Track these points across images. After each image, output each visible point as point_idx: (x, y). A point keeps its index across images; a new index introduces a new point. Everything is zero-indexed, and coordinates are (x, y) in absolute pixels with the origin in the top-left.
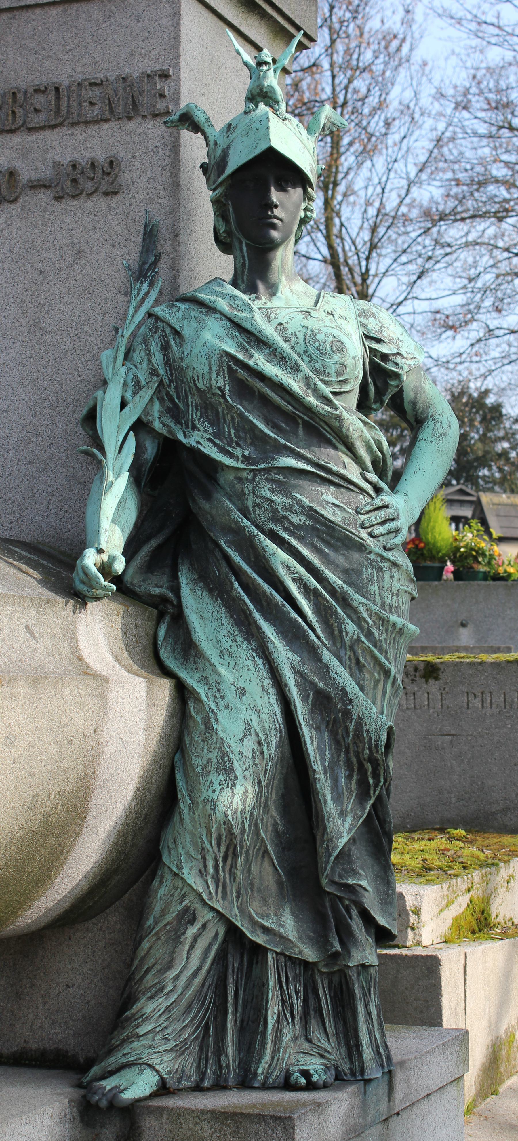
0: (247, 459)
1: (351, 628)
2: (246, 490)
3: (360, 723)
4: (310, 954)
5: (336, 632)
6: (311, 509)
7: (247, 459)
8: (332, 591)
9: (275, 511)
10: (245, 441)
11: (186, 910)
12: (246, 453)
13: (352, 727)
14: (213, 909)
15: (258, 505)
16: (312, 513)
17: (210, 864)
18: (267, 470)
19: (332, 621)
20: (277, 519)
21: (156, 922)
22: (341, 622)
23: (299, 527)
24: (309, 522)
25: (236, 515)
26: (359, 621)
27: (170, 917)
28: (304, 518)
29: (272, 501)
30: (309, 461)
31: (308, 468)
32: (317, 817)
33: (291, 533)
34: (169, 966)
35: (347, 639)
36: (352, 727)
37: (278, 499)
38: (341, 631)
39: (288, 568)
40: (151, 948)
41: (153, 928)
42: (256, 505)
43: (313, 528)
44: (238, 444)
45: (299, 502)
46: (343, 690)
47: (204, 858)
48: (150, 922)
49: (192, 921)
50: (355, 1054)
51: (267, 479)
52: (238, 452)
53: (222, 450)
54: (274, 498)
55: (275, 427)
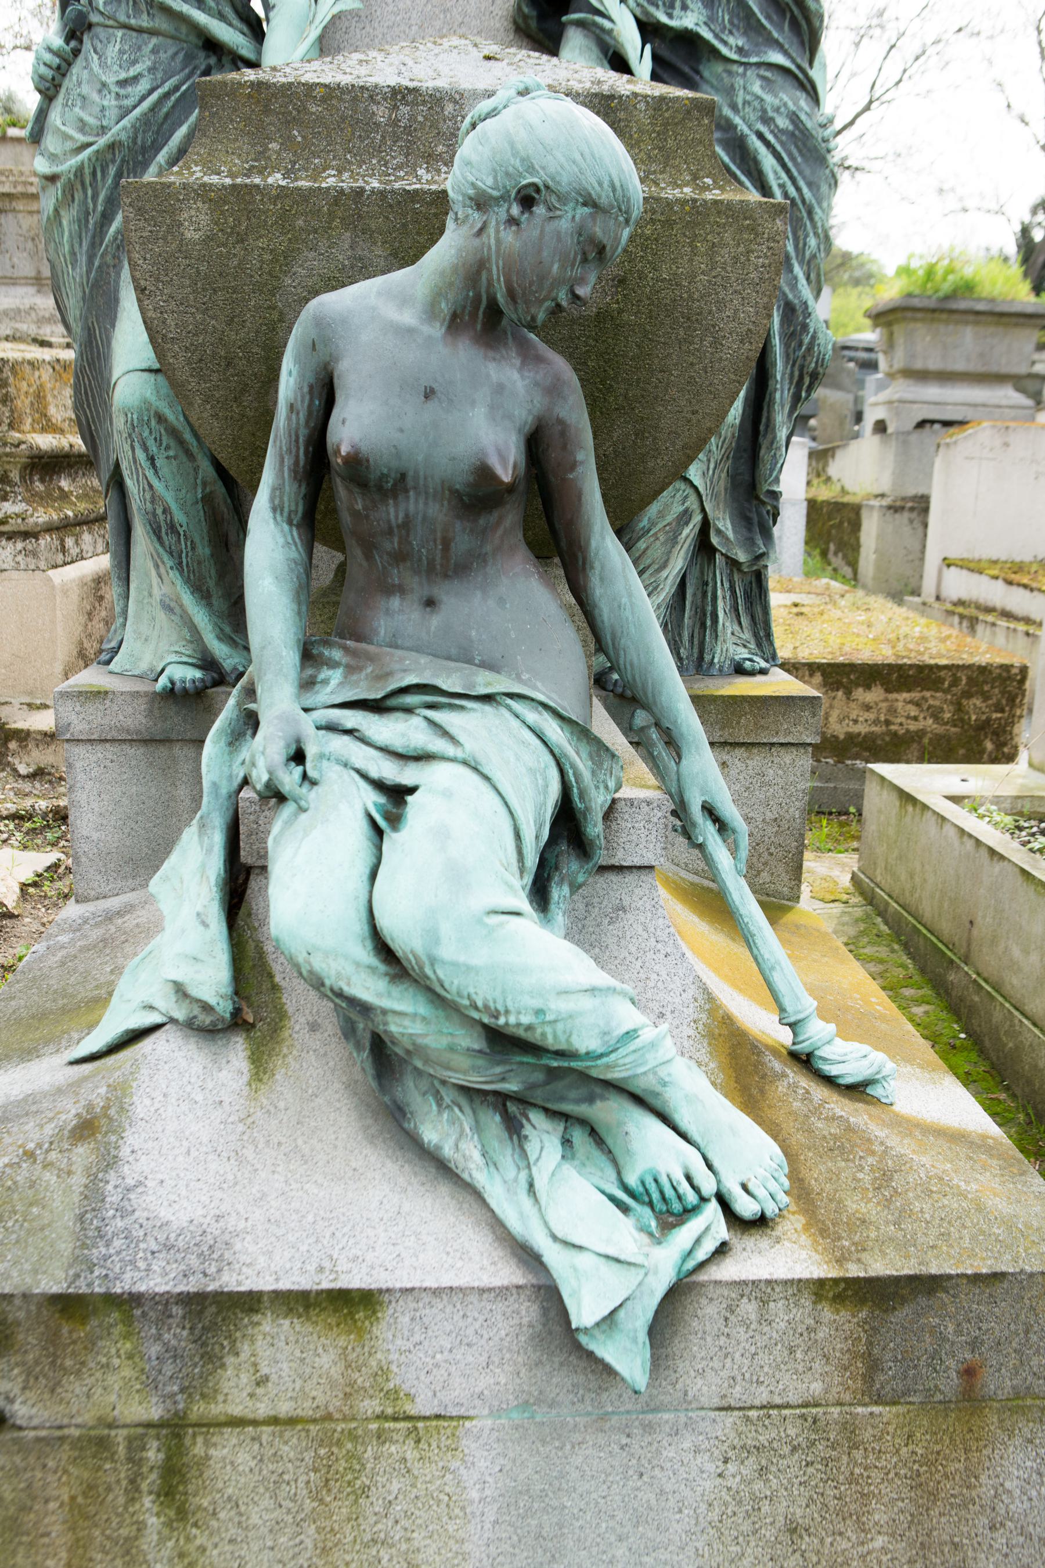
0: (740, 50)
1: (812, 242)
2: (737, 86)
3: (814, 337)
4: (742, 556)
5: (801, 245)
6: (794, 113)
7: (740, 50)
8: (804, 201)
9: (764, 111)
10: (738, 29)
11: (686, 511)
12: (740, 44)
13: (807, 340)
14: (703, 510)
15: (749, 103)
16: (794, 118)
17: (712, 466)
18: (759, 65)
19: (800, 233)
20: (766, 120)
21: (653, 524)
22: (807, 236)
23: (782, 131)
24: (791, 128)
25: (727, 112)
26: (816, 234)
27: (669, 518)
28: (787, 122)
29: (762, 100)
30: (793, 61)
31: (793, 67)
32: (767, 426)
33: (776, 136)
34: (664, 566)
35: (808, 254)
36: (807, 340)
37: (768, 98)
38: (805, 244)
39: (776, 173)
40: (647, 548)
41: (649, 530)
42: (745, 102)
43: (793, 134)
44: (731, 32)
45: (785, 104)
46: (805, 303)
47: (709, 460)
48: (645, 522)
49: (687, 524)
50: (765, 643)
51: (758, 75)
52: (731, 40)
53: (716, 36)
54: (765, 96)
55: (768, 17)
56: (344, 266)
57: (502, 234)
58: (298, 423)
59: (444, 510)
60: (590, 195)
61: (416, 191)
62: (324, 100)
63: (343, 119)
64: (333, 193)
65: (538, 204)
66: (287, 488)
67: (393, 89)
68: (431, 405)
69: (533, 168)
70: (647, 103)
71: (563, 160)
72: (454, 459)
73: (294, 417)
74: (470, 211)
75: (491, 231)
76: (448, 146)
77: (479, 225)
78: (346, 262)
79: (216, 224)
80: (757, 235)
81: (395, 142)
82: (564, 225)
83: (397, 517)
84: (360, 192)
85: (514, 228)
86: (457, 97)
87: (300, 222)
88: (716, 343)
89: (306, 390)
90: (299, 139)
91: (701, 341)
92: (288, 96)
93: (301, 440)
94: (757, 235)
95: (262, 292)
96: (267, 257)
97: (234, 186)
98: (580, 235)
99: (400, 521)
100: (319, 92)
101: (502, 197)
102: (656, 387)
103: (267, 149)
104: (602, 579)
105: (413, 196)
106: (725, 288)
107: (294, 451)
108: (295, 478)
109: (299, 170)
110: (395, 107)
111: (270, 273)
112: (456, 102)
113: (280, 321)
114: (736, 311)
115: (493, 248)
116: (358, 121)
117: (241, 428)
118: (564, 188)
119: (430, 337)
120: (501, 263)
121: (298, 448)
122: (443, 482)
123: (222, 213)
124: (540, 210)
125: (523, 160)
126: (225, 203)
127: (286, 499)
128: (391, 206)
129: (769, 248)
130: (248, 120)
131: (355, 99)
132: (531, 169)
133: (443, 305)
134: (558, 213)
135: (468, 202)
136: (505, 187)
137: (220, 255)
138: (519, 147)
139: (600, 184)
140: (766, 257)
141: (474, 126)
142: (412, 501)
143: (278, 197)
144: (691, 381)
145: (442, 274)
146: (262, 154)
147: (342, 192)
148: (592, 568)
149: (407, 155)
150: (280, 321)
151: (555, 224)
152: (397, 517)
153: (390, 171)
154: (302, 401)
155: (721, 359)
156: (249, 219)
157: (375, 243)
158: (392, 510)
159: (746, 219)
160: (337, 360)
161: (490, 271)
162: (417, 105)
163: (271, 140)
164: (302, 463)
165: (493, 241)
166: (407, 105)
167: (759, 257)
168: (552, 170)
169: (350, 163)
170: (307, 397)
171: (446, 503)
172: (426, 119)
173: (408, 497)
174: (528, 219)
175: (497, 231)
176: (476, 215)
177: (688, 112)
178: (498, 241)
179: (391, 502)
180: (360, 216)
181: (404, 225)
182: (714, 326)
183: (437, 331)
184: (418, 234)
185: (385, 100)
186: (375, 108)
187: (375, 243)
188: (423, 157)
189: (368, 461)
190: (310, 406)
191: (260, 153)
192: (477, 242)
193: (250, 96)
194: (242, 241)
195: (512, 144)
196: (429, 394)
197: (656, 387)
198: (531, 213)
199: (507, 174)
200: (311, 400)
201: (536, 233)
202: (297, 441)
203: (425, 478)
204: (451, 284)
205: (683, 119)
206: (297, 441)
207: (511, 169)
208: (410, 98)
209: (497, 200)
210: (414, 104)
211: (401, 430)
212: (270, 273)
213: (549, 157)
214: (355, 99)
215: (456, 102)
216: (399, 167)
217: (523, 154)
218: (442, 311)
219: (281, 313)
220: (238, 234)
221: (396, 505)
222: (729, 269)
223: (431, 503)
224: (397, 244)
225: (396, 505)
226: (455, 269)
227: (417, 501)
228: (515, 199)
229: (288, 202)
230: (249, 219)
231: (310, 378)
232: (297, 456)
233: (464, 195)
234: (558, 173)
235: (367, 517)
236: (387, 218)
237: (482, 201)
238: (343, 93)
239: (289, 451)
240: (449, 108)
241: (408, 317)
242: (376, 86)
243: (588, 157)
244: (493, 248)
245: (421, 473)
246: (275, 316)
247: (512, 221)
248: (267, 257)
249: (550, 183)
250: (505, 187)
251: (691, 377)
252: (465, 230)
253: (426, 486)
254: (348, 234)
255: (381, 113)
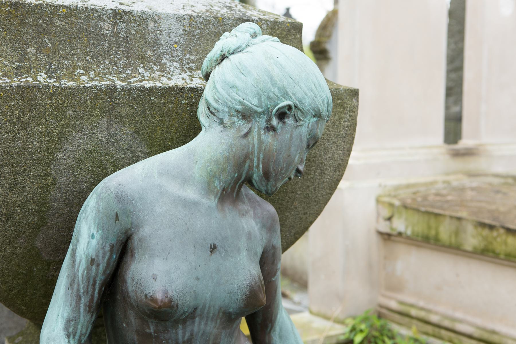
56: (102, 142)
57: (263, 137)
58: (97, 272)
59: (217, 326)
60: (319, 110)
61: (151, 88)
62: (65, 17)
63: (81, 31)
64: (95, 90)
65: (288, 117)
66: (82, 319)
67: (115, 11)
68: (216, 256)
69: (288, 94)
70: (267, 24)
71: (305, 89)
72: (231, 292)
73: (94, 268)
74: (236, 119)
75: (255, 134)
76: (154, 51)
77: (246, 130)
78: (104, 139)
79: (4, 116)
80: (344, 108)
81: (118, 48)
82: (304, 130)
83: (184, 336)
84: (112, 89)
85: (271, 133)
86: (157, 18)
87: (71, 112)
88: (322, 173)
89: (107, 248)
90: (50, 45)
91: (315, 172)
92: (39, 13)
93: (97, 284)
94: (344, 108)
95: (40, 164)
96: (45, 139)
97: (19, 87)
98: (309, 135)
99: (186, 338)
100: (62, 12)
101: (263, 112)
102: (288, 202)
103: (26, 53)
104: (280, 337)
105: (150, 91)
106: (328, 141)
107: (90, 292)
108: (89, 311)
109: (55, 69)
110: (115, 24)
111: (47, 151)
112: (156, 21)
113: (52, 184)
114: (333, 154)
115: (256, 145)
116: (91, 33)
117: (10, 261)
118: (307, 107)
119: (209, 207)
120: (261, 156)
121: (94, 289)
122: (220, 308)
123: (10, 107)
124: (290, 121)
125: (280, 89)
126: (12, 100)
127: (79, 327)
128: (135, 99)
129: (350, 116)
130: (8, 30)
131: (88, 18)
132: (286, 95)
133: (217, 184)
134: (301, 123)
135: (235, 113)
136: (266, 106)
137: (8, 139)
138: (277, 79)
139: (323, 103)
140: (349, 121)
141: (223, 58)
142: (196, 324)
143: (53, 94)
144: (307, 197)
145: (217, 162)
146: (23, 56)
147: (100, 90)
148: (275, 331)
149: (128, 57)
150: (52, 184)
151: (299, 130)
152: (184, 336)
153: (121, 70)
154: (103, 257)
155: (324, 182)
156: (31, 111)
157: (124, 125)
158: (180, 332)
159: (338, 99)
160: (138, 227)
161: (252, 160)
162: (130, 22)
163: (29, 45)
164: (95, 300)
165: (256, 141)
166: (123, 22)
167: (345, 121)
168: (300, 95)
169: (90, 63)
170: (108, 254)
171: (218, 321)
172: (137, 32)
173: (194, 322)
174: (282, 128)
175: (259, 135)
176: (241, 122)
177: (289, 31)
178: (260, 142)
179: (180, 326)
180: (113, 106)
181: (144, 112)
182: (322, 164)
183: (212, 202)
184: (153, 117)
185: (109, 18)
186: (102, 24)
187: (124, 125)
188: (138, 59)
189: (177, 306)
190: (109, 259)
191: (21, 55)
192: (244, 141)
193: (9, 12)
194: (26, 128)
195: (271, 78)
196: (213, 248)
197: (288, 202)
198: (284, 123)
199: (269, 97)
200: (111, 255)
201: (288, 136)
202: (94, 285)
203: (209, 308)
204: (223, 170)
205: (287, 35)
206: (94, 285)
207: (272, 95)
208: (126, 18)
209: (259, 114)
210: (128, 22)
211: (198, 279)
212: (47, 151)
213: (297, 87)
214: (88, 18)
215: (156, 21)
216: (125, 67)
217: (280, 84)
218: (216, 187)
219: (54, 179)
220: (22, 123)
221: (184, 328)
222: (331, 129)
223: (209, 323)
224: (139, 125)
225: (184, 328)
226: (227, 159)
227: (200, 323)
228: (275, 115)
229: (60, 97)
230: (31, 111)
231: (112, 240)
232: (93, 296)
233: (230, 108)
234: (303, 98)
235: (157, 338)
236: (132, 107)
237: (248, 114)
238: (79, 13)
239: (86, 292)
240: (151, 25)
241: (191, 193)
242: (103, 9)
243: (317, 86)
244: (256, 145)
245: (207, 305)
246: (49, 181)
247: (270, 128)
248: (45, 139)
249: (299, 105)
250: (266, 106)
251: (307, 194)
252: (232, 132)
253: (208, 313)
254: (105, 119)
255: (107, 27)
